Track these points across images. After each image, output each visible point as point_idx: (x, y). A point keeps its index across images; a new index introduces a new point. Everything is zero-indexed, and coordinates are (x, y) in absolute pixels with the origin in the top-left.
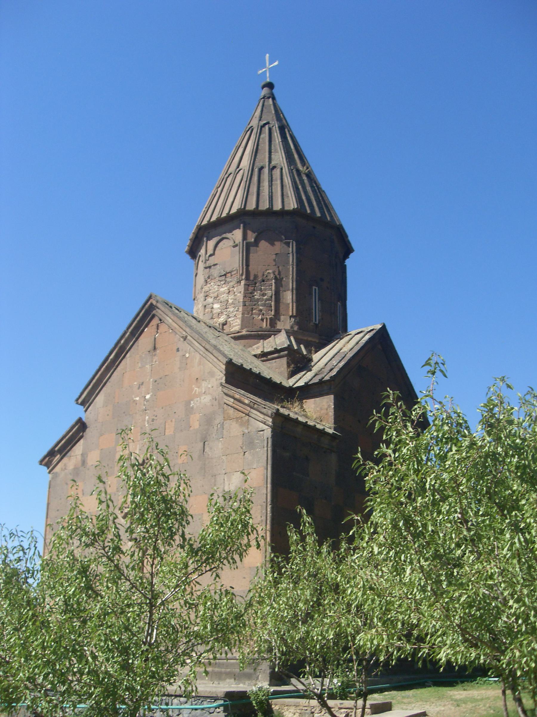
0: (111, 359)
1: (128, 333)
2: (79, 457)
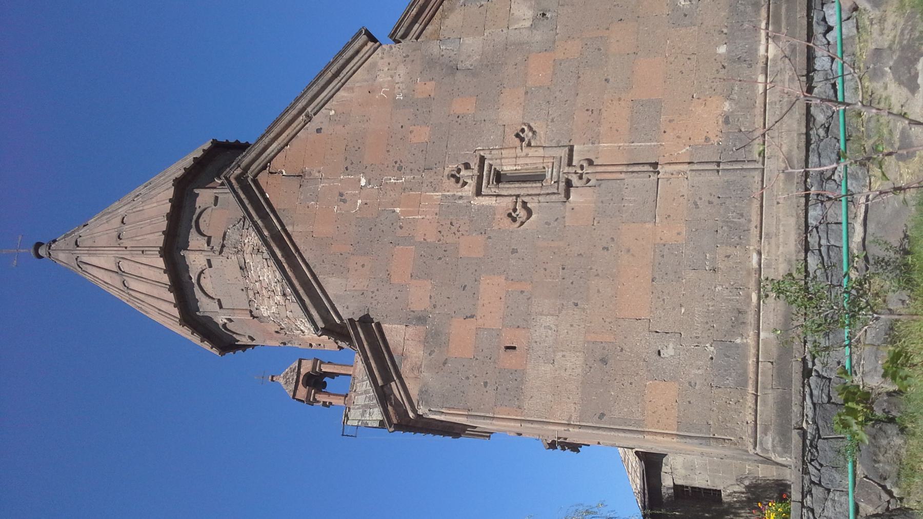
0: (283, 256)
1: (259, 222)
2: (411, 330)
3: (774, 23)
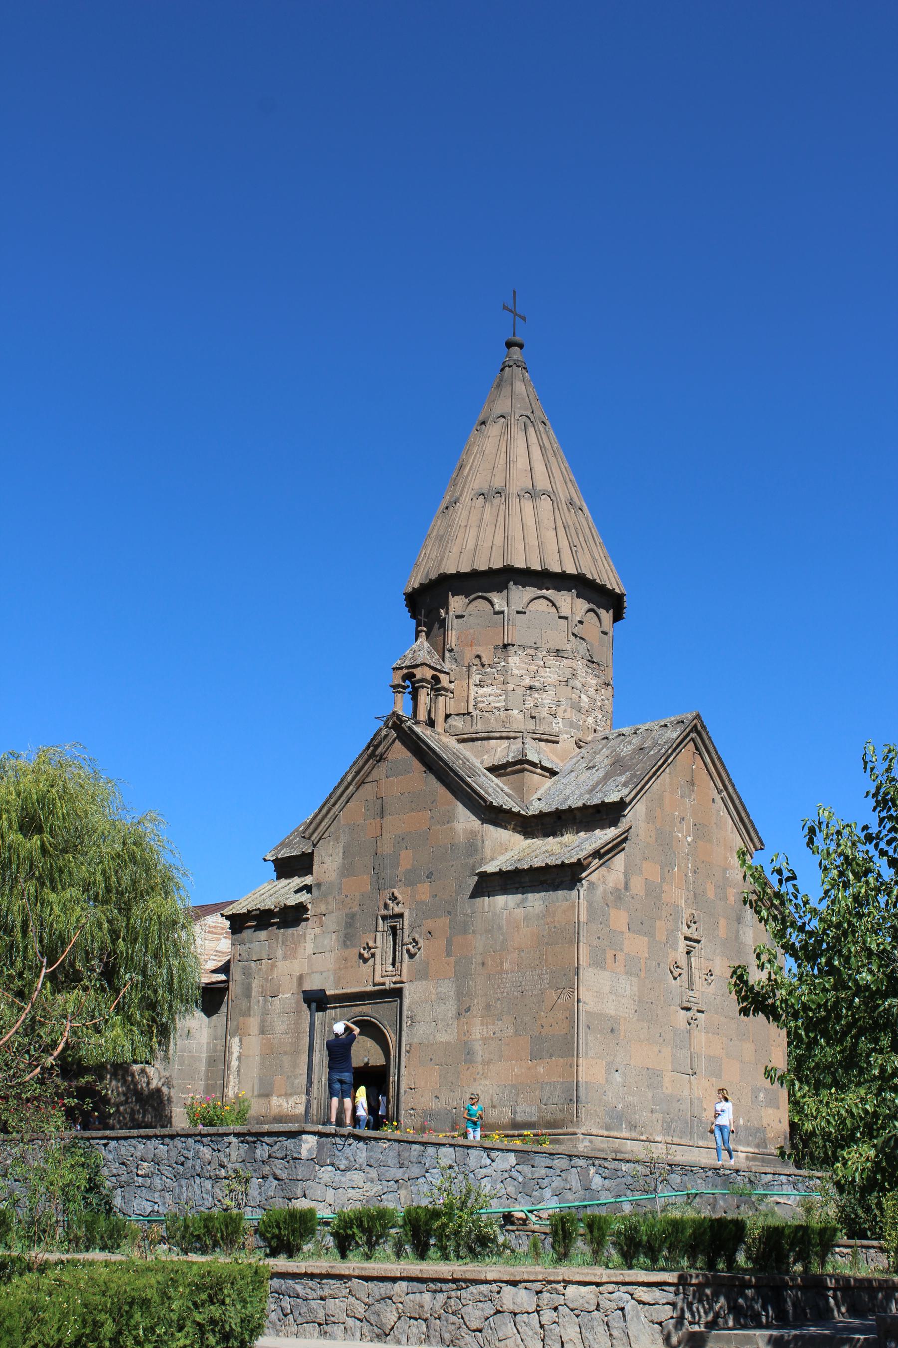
2: (622, 877)
3: (753, 1157)
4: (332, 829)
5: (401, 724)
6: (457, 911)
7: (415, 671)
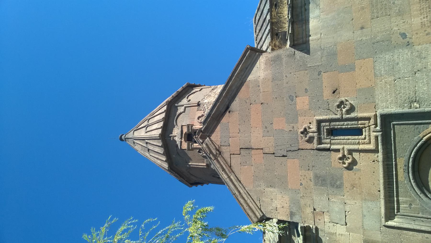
4: (255, 198)
5: (201, 131)
6: (318, 66)
7: (184, 132)
